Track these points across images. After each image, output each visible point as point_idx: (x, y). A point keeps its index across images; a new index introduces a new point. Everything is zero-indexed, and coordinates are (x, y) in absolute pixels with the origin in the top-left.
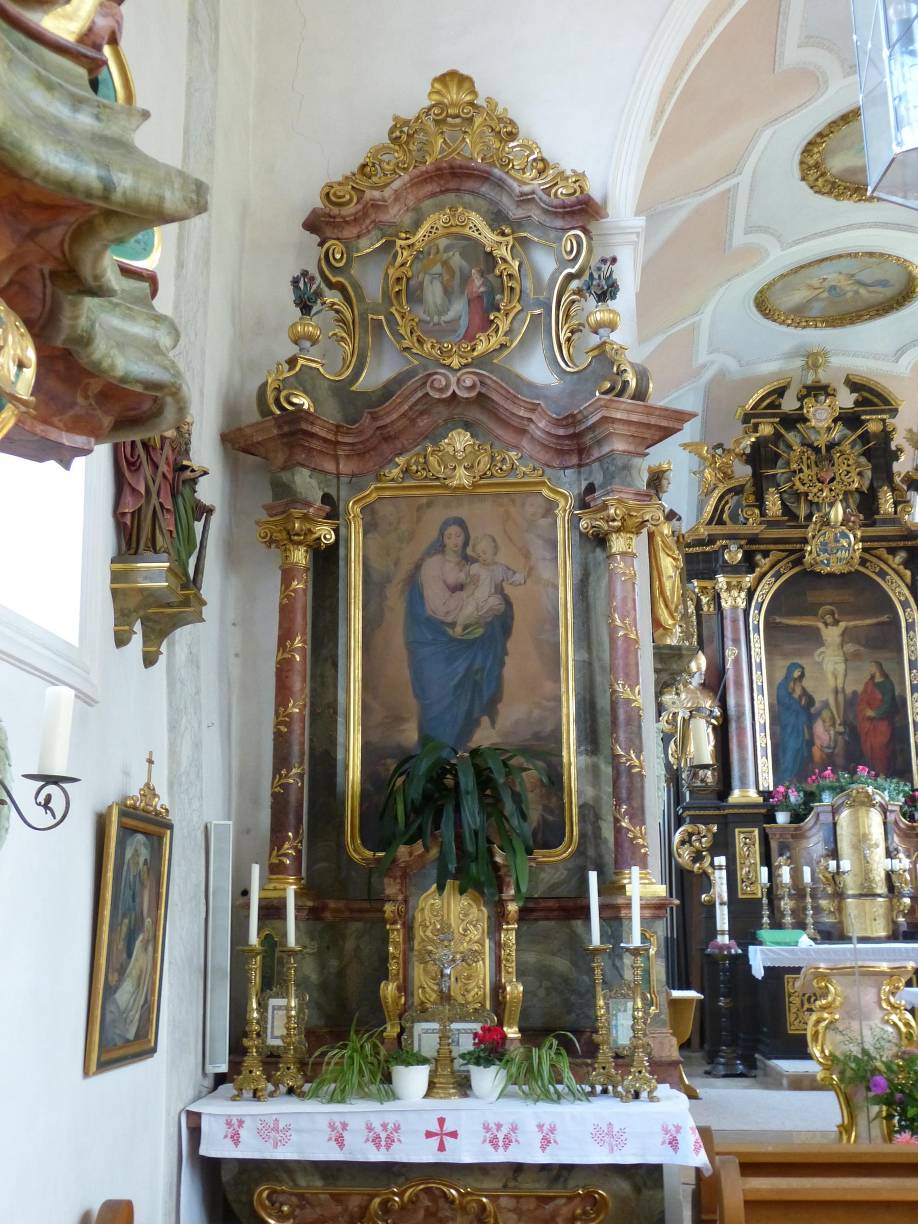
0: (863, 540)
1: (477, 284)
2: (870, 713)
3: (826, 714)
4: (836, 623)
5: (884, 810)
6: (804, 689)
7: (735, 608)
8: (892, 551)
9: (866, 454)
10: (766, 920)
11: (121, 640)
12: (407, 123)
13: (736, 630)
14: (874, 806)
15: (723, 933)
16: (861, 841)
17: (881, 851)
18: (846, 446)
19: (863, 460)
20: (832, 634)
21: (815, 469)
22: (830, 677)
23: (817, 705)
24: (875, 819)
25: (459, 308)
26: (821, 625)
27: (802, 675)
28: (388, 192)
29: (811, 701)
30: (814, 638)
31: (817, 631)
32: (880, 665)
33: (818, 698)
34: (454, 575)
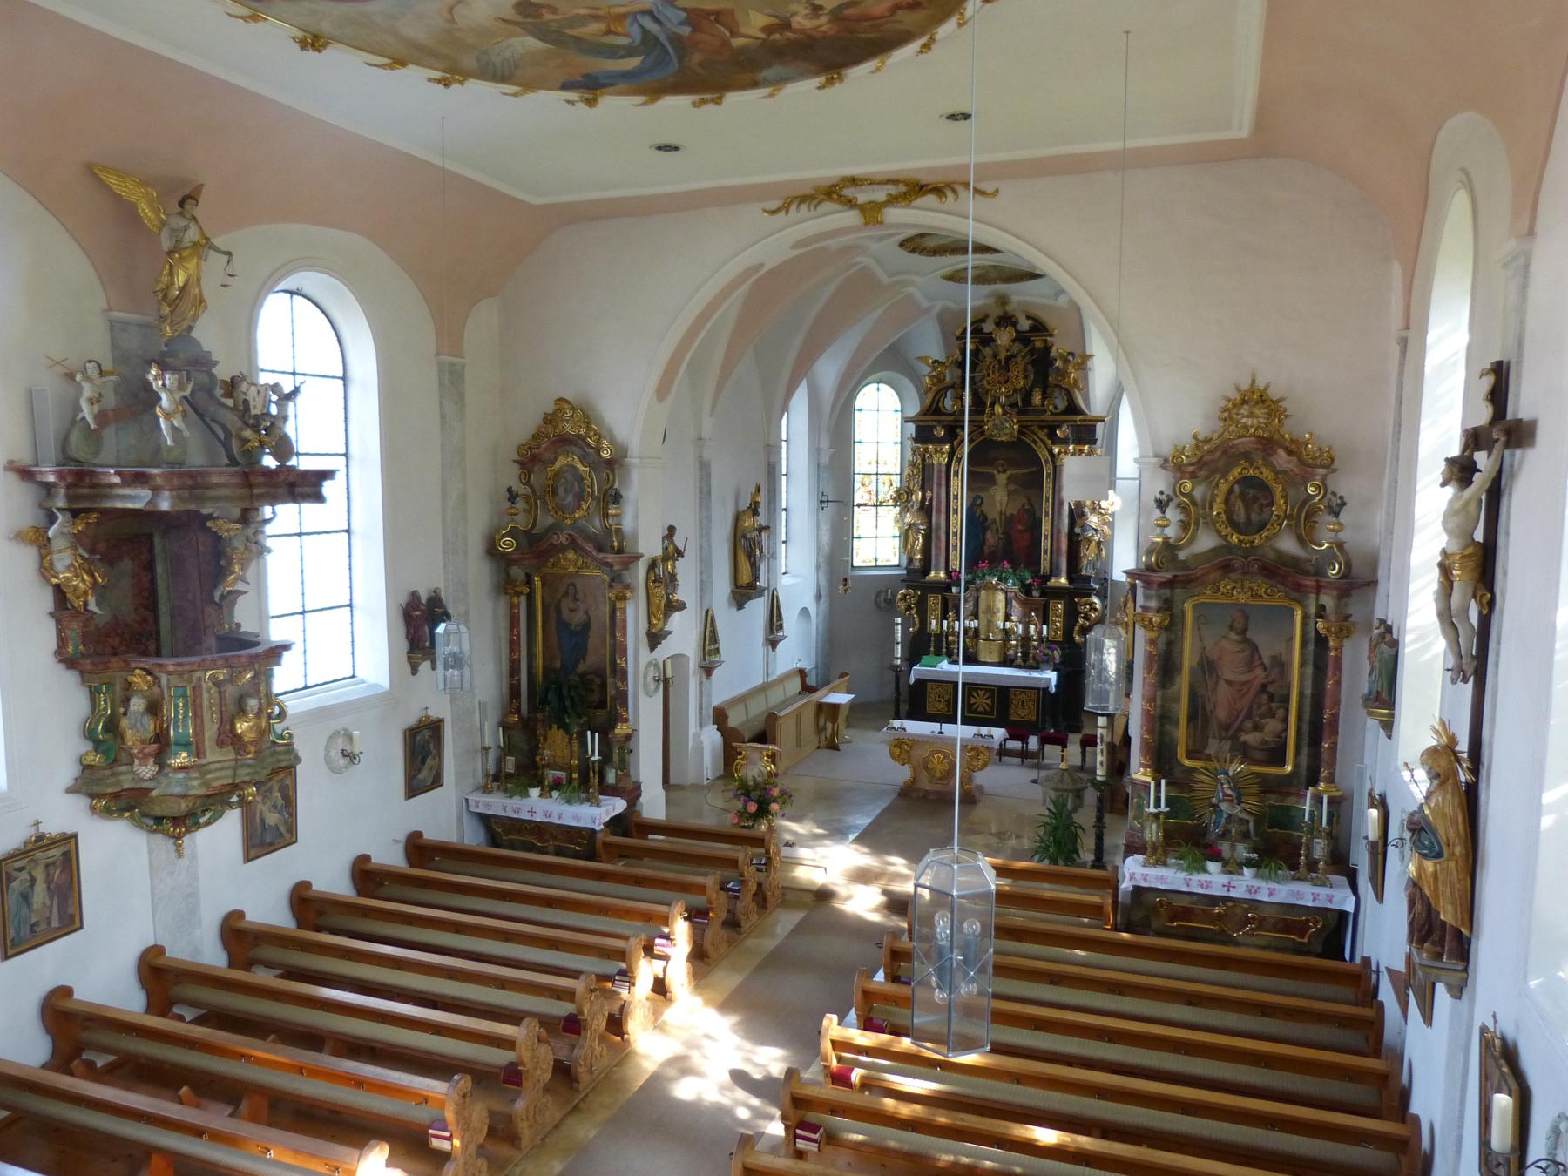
0: (1018, 422)
1: (576, 487)
2: (1020, 527)
3: (994, 527)
4: (1005, 471)
5: (1005, 592)
6: (982, 512)
7: (940, 464)
8: (1041, 428)
9: (1033, 363)
10: (932, 649)
11: (414, 671)
12: (550, 415)
13: (939, 478)
14: (997, 590)
15: (897, 658)
16: (991, 611)
17: (1001, 614)
18: (1019, 359)
19: (1030, 367)
20: (1002, 478)
21: (997, 374)
22: (998, 504)
23: (989, 521)
24: (1001, 597)
25: (570, 498)
26: (995, 472)
27: (982, 502)
28: (541, 450)
29: (986, 519)
30: (991, 480)
31: (994, 475)
32: (1028, 499)
33: (990, 517)
34: (572, 606)
